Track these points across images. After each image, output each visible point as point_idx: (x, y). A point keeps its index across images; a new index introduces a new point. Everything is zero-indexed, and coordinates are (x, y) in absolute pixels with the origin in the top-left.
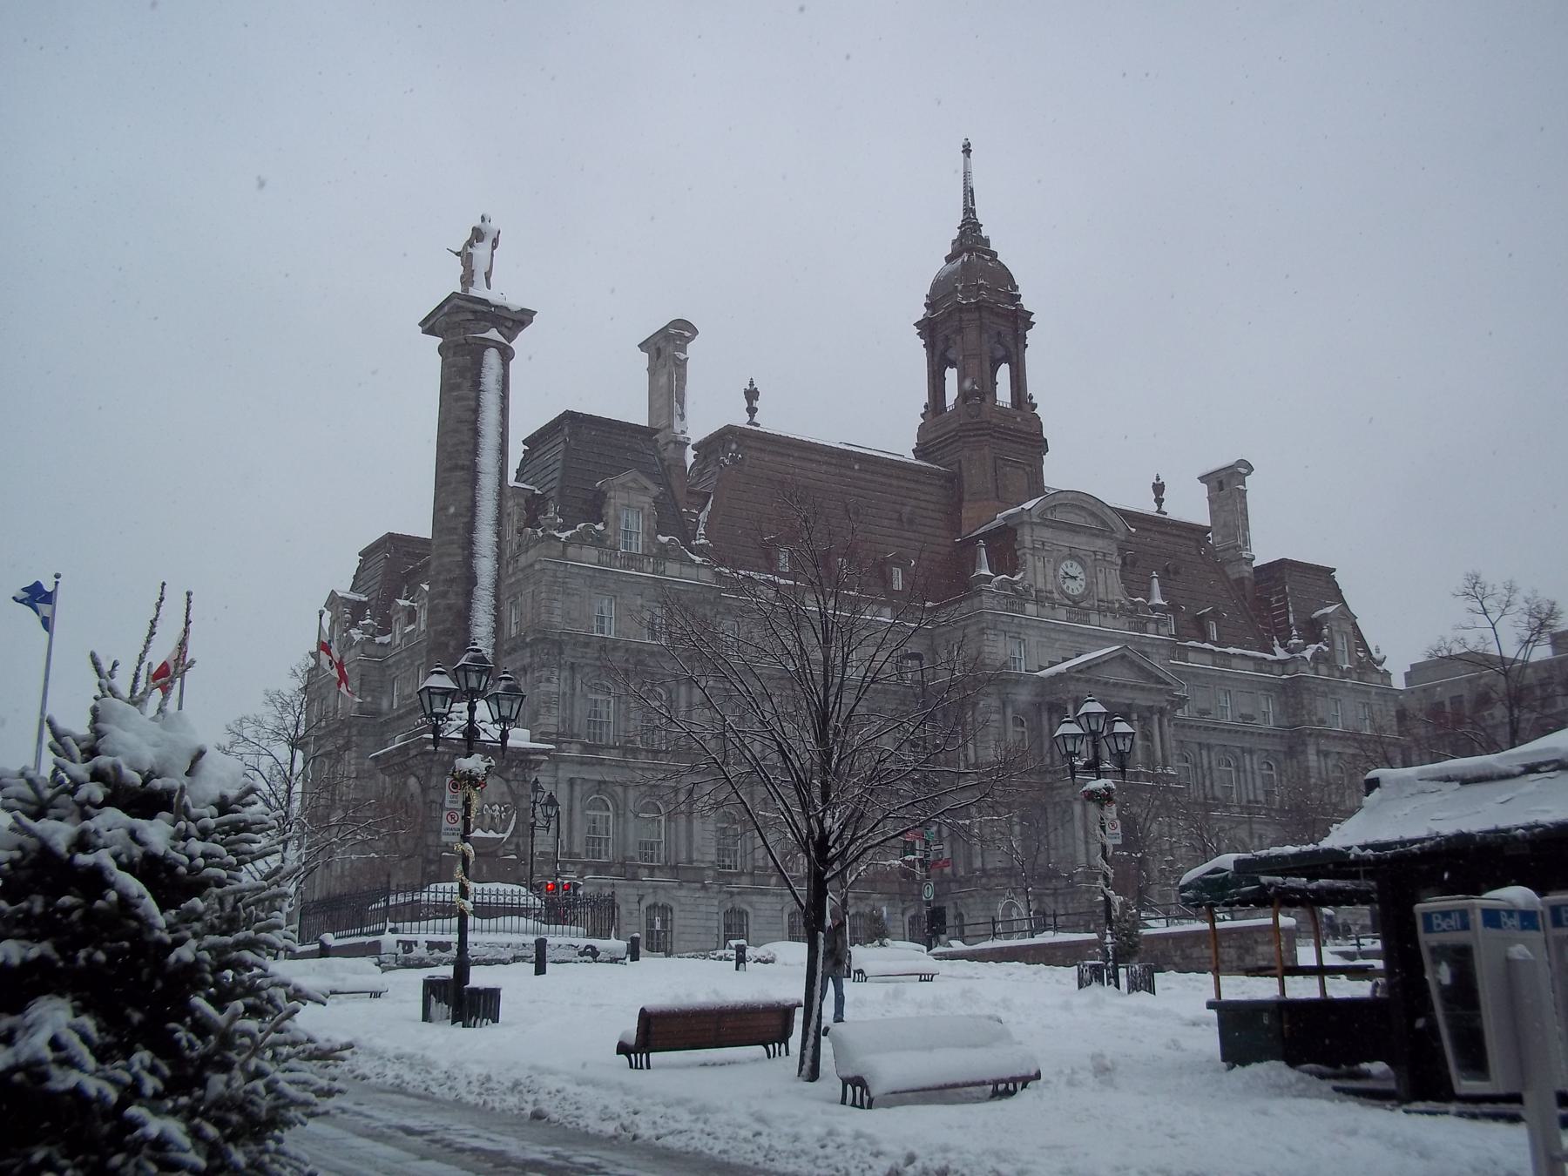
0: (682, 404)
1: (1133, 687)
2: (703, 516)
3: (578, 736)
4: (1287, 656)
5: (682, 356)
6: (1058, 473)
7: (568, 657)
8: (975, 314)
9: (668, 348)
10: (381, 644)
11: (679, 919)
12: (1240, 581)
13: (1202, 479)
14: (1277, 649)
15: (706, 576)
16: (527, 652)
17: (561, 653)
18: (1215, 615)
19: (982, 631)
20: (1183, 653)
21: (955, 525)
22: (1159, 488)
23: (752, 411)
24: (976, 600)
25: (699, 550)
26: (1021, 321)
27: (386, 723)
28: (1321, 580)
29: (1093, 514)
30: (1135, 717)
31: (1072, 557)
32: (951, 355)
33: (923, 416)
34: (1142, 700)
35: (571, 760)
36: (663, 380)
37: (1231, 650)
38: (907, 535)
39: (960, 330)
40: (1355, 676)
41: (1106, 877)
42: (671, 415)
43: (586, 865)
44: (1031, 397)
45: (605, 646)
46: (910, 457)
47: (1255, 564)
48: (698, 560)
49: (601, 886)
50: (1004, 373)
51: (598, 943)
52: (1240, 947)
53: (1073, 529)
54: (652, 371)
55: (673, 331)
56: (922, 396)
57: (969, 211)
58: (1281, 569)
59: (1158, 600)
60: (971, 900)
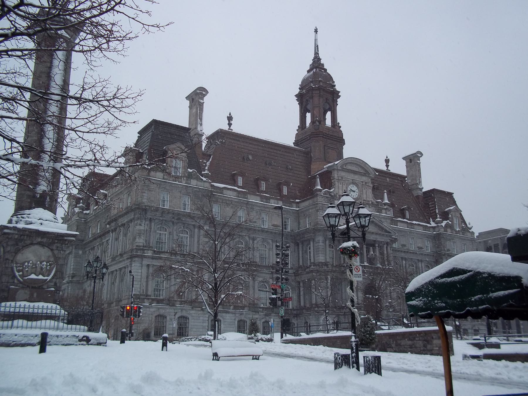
0: (201, 119)
1: (376, 234)
2: (208, 164)
3: (152, 247)
4: (436, 225)
5: (202, 101)
6: (348, 152)
7: (149, 215)
8: (318, 92)
9: (196, 98)
10: (86, 214)
11: (192, 323)
12: (418, 197)
13: (404, 158)
14: (432, 222)
15: (207, 185)
16: (133, 214)
17: (146, 213)
18: (409, 209)
19: (317, 211)
20: (396, 223)
21: (309, 172)
22: (387, 161)
23: (230, 125)
24: (315, 199)
25: (206, 176)
26: (335, 95)
27: (86, 244)
28: (448, 197)
30: (377, 245)
31: (353, 183)
32: (309, 107)
33: (297, 130)
34: (379, 239)
35: (148, 257)
36: (194, 111)
37: (414, 222)
38: (290, 174)
39: (312, 97)
40: (461, 233)
41: (352, 301)
42: (196, 124)
43: (153, 300)
44: (339, 124)
45: (164, 212)
46: (293, 145)
47: (424, 190)
48: (204, 179)
49: (159, 309)
50: (329, 115)
51: (91, 335)
52: (425, 340)
53: (355, 173)
54: (191, 107)
55: (198, 91)
56: (297, 123)
57: (316, 53)
59: (386, 201)
60: (311, 317)
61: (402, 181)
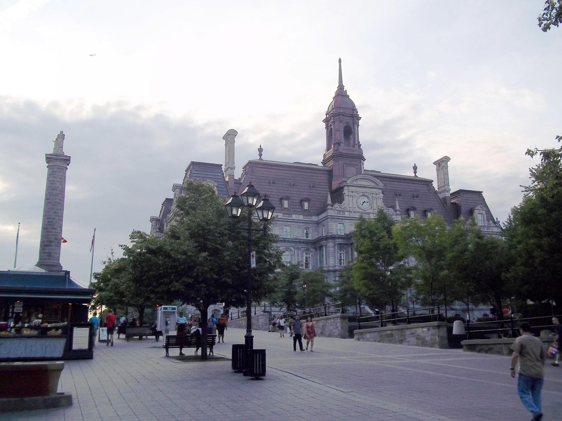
13: (435, 163)
22: (415, 168)
29: (372, 181)
47: (451, 192)
58: (460, 192)
61: (428, 185)
